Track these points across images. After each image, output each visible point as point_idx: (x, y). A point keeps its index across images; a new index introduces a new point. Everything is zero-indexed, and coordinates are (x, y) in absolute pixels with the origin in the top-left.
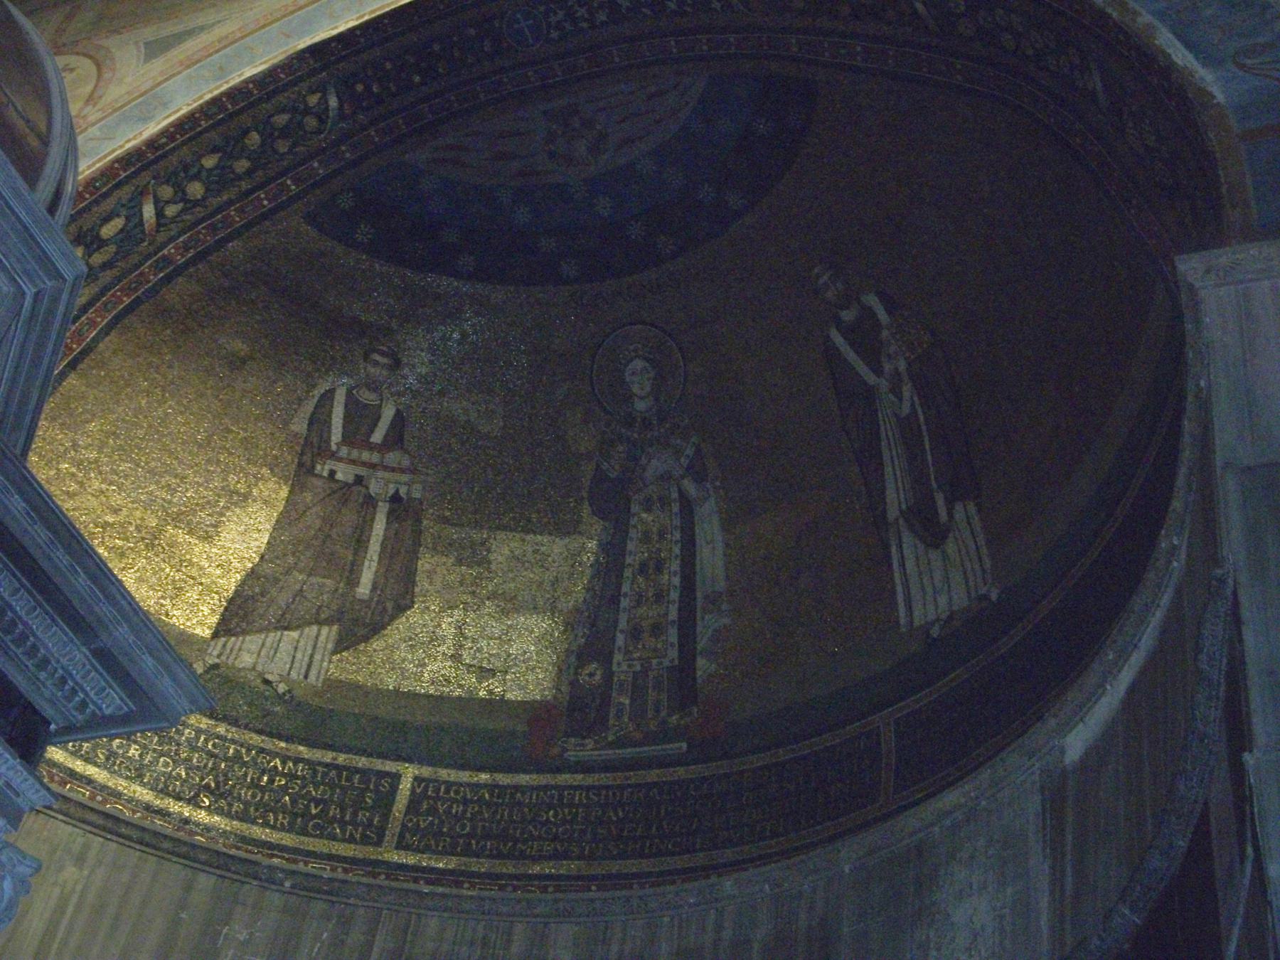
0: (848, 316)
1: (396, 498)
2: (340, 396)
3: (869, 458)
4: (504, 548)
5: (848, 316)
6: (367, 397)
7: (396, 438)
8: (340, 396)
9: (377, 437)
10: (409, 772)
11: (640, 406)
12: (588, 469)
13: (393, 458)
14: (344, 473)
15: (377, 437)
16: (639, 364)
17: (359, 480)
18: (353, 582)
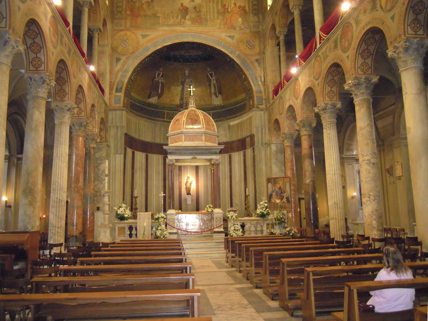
0: (210, 73)
1: (162, 82)
2: (157, 72)
3: (210, 85)
4: (173, 88)
5: (210, 73)
6: (159, 72)
7: (162, 76)
8: (157, 72)
9: (160, 76)
10: (166, 111)
11: (187, 75)
12: (180, 80)
13: (161, 78)
14: (157, 80)
15: (160, 76)
16: (187, 71)
17: (158, 80)
18: (158, 92)
